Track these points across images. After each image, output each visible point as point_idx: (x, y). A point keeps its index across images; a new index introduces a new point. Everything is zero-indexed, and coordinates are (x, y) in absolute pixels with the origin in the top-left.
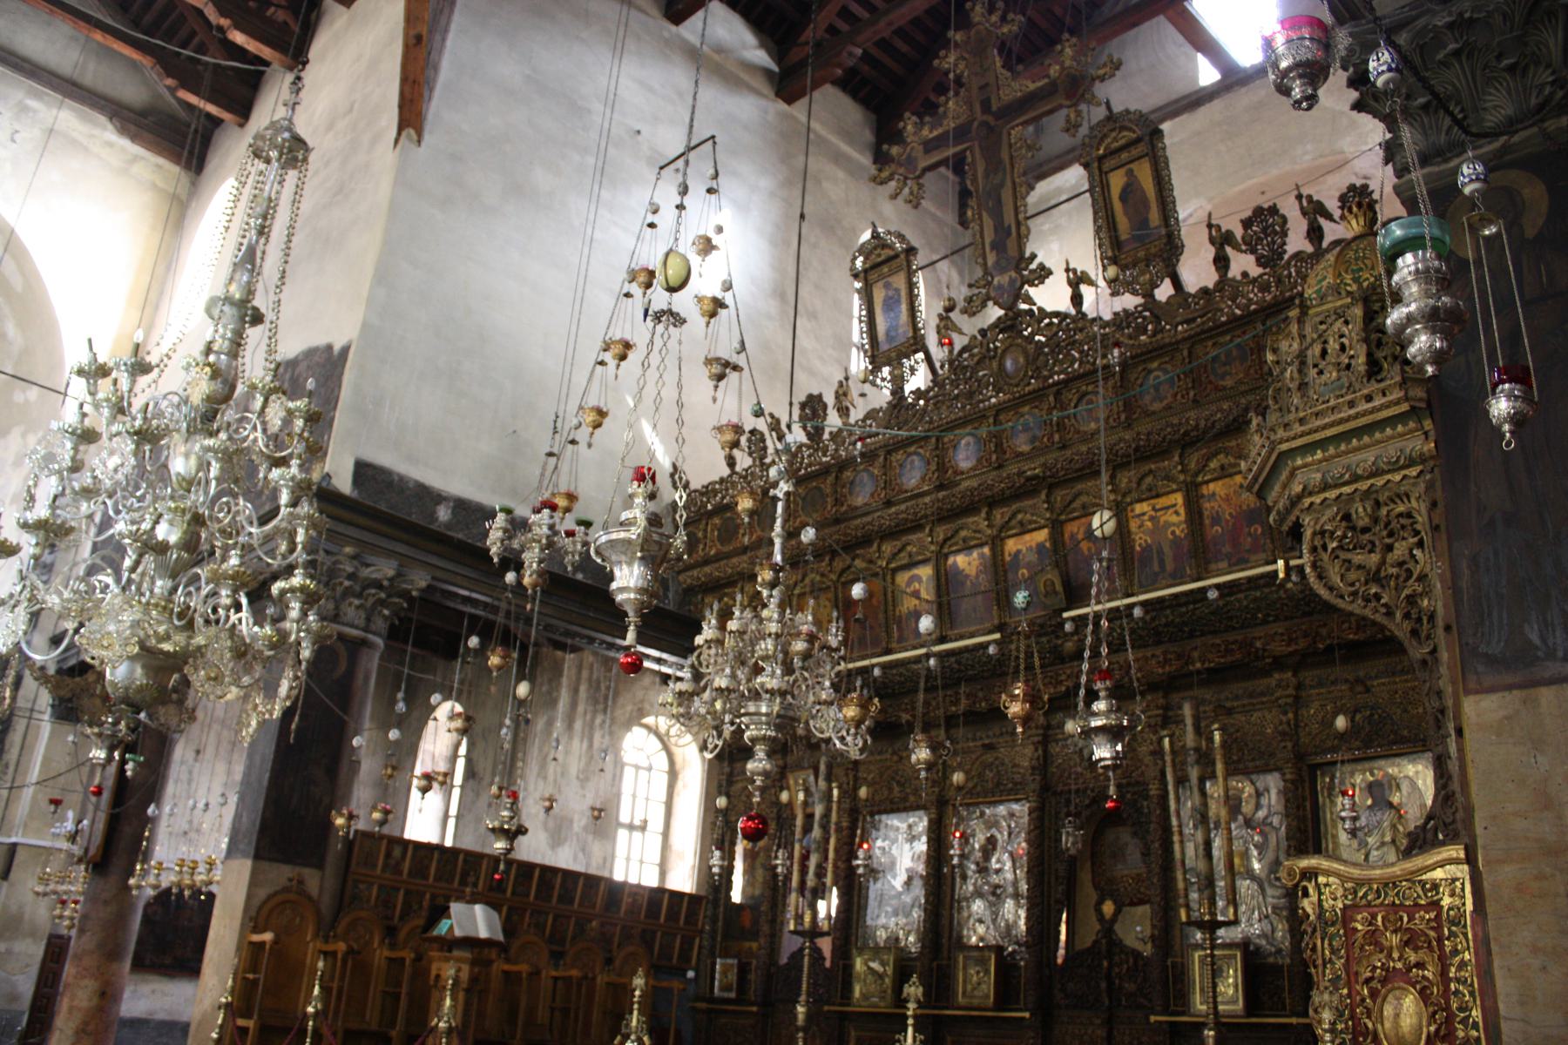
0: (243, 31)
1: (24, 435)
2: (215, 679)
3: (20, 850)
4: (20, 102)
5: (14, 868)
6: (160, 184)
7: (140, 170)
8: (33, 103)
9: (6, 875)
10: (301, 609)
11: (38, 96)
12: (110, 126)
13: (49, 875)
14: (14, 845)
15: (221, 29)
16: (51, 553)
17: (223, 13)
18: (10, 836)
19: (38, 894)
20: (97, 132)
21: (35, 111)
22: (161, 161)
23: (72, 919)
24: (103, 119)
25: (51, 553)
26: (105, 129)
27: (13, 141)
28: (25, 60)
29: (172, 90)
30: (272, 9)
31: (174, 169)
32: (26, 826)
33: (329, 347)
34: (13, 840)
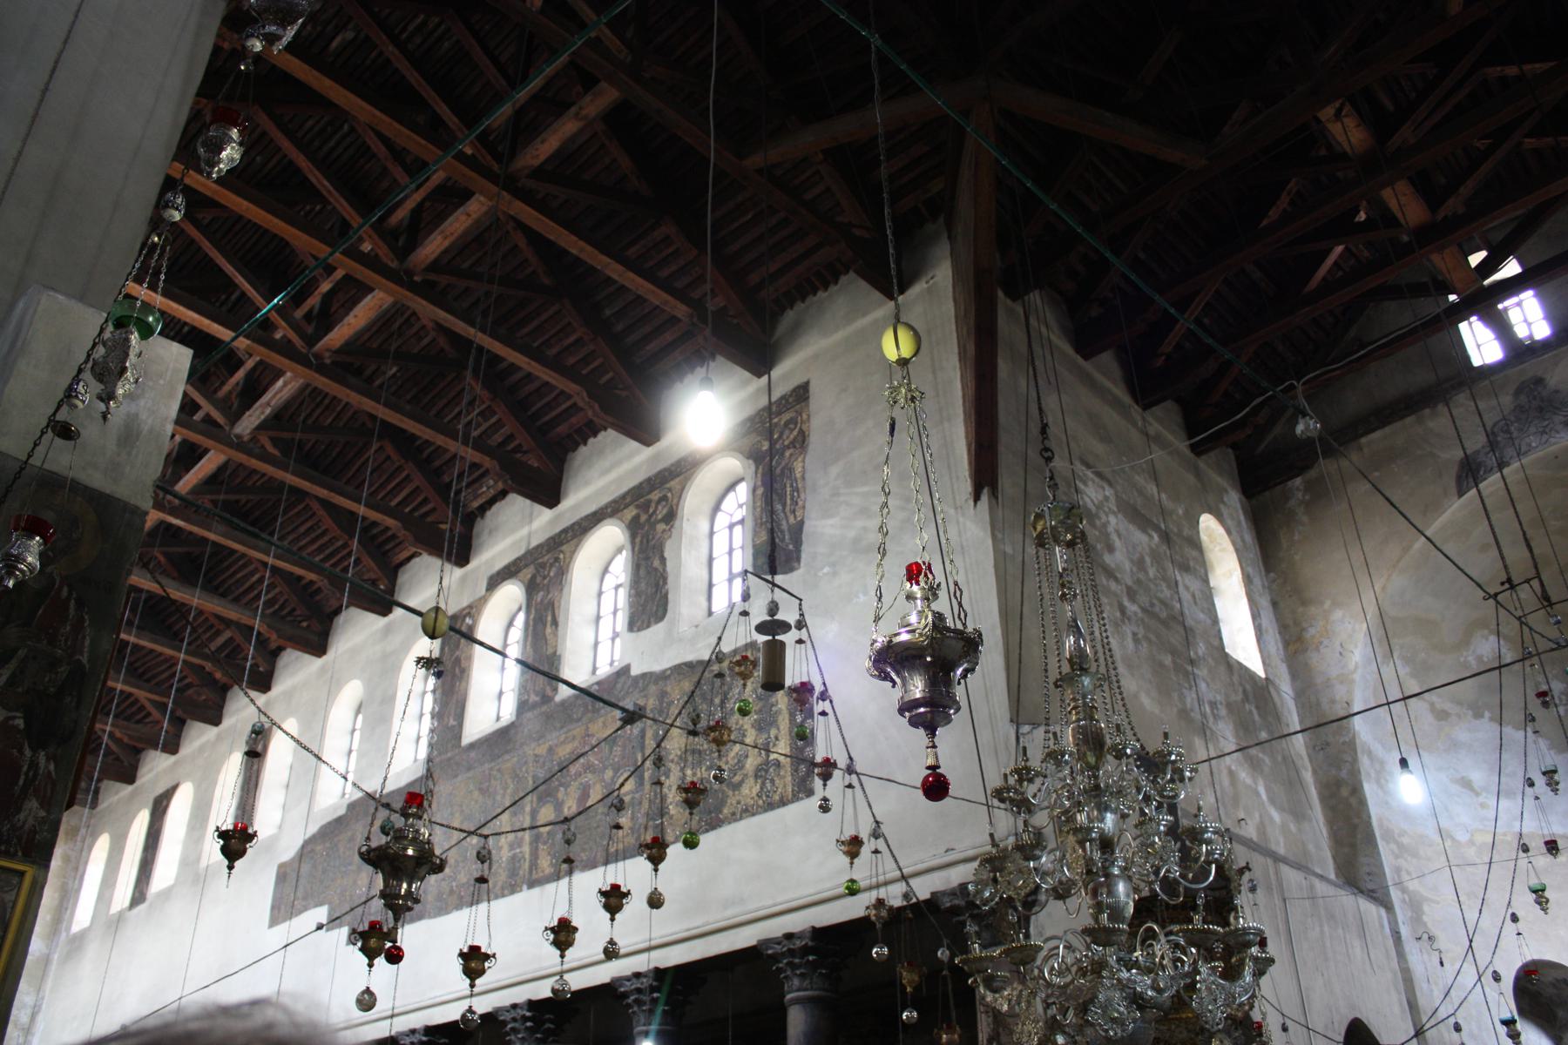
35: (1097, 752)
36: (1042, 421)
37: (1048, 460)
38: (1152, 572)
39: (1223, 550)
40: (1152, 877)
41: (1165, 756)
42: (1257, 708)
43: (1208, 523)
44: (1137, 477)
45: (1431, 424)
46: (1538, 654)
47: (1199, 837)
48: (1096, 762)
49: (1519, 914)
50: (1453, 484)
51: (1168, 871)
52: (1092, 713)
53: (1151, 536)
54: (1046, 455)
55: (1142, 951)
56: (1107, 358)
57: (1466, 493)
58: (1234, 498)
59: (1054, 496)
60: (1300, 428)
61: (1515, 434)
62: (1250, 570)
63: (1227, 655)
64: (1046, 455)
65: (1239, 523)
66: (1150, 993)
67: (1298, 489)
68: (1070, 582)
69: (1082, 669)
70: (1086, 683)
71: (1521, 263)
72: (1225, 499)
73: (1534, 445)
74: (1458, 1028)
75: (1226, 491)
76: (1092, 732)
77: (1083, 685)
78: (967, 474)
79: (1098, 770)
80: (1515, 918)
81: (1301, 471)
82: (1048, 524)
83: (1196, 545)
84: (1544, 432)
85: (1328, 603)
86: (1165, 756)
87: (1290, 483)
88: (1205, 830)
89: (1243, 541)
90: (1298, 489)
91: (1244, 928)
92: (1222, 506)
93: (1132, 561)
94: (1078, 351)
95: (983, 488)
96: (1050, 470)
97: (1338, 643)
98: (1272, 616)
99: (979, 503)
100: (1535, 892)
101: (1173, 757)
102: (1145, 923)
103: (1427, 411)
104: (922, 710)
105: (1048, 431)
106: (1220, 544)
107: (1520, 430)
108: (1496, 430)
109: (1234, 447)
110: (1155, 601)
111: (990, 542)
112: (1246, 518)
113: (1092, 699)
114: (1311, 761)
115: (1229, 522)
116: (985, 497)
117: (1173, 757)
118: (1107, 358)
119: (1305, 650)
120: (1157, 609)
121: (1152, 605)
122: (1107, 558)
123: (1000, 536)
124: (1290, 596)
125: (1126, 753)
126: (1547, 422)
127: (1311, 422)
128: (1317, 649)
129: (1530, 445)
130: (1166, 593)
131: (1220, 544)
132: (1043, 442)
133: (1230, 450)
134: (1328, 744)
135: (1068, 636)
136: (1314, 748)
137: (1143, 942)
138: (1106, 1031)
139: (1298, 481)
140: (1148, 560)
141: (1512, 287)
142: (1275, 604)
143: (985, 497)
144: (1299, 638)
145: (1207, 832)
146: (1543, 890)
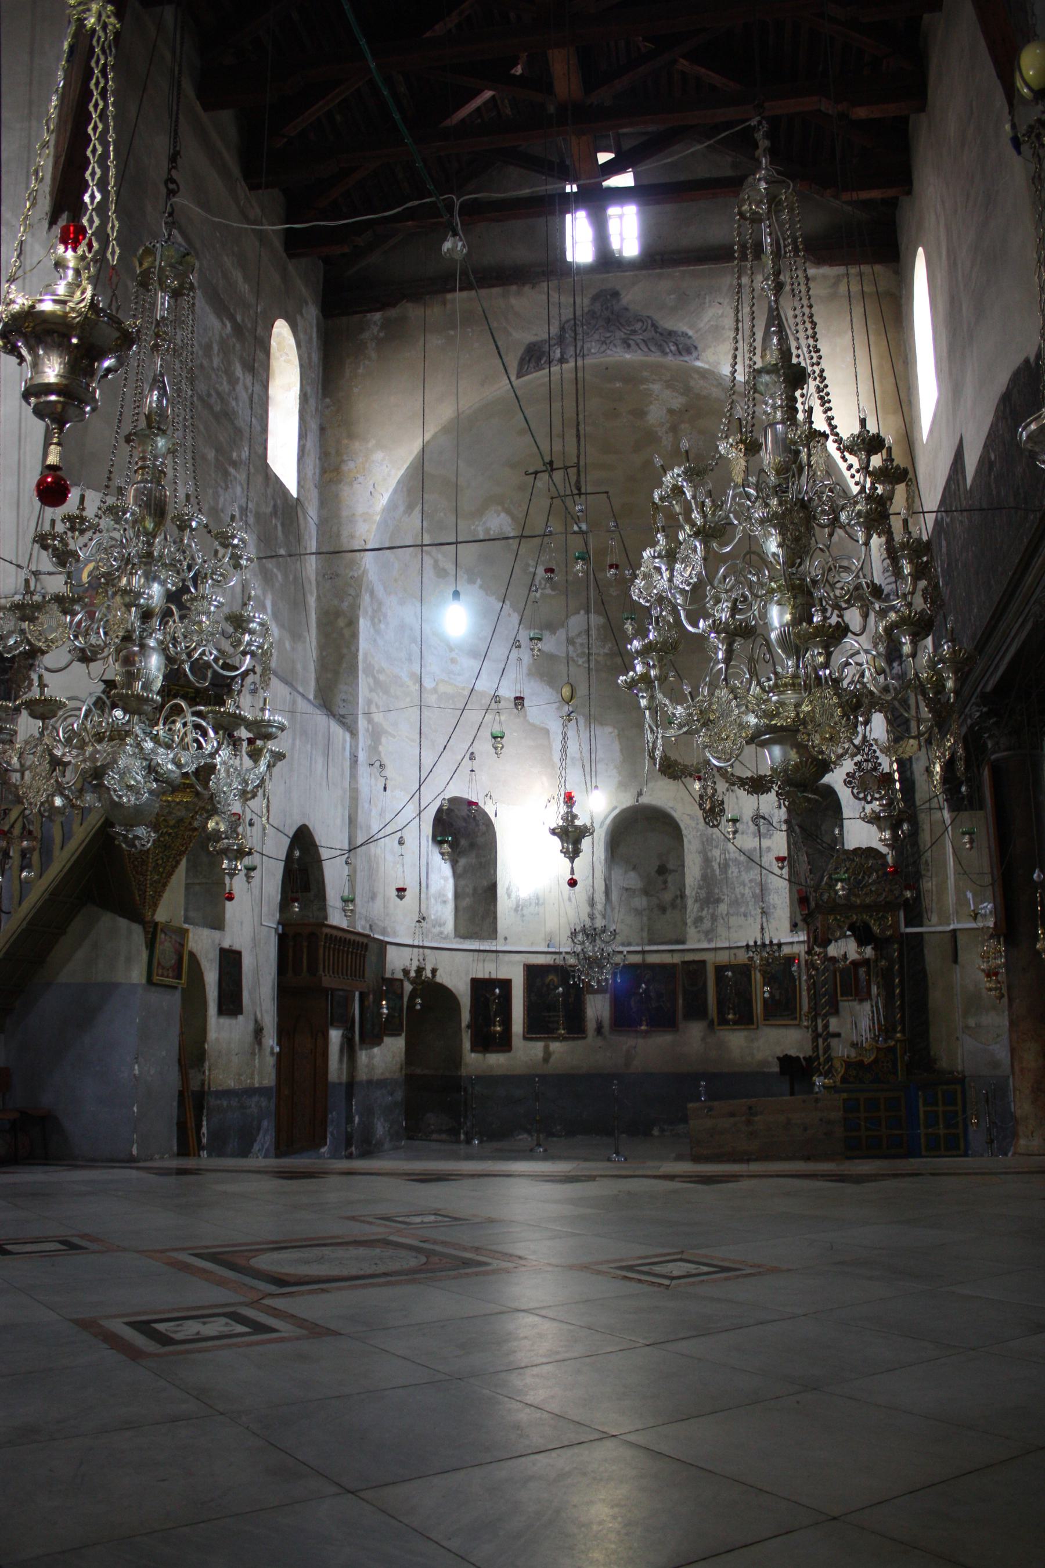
2: (831, 739)
3: (959, 936)
5: (960, 952)
10: (912, 642)
14: (954, 931)
18: (949, 924)
25: (900, 664)
32: (957, 913)
33: (1027, 361)
34: (952, 927)
35: (157, 519)
36: (175, 147)
37: (171, 193)
38: (216, 361)
39: (288, 361)
40: (184, 657)
41: (228, 538)
42: (283, 525)
44: (226, 259)
45: (513, 301)
47: (244, 625)
48: (154, 529)
49: (477, 755)
51: (203, 653)
52: (160, 477)
54: (172, 186)
55: (164, 724)
56: (227, 116)
57: (523, 376)
58: (312, 312)
59: (170, 235)
60: (447, 245)
62: (309, 389)
63: (267, 466)
64: (172, 186)
65: (311, 339)
66: (170, 766)
67: (375, 323)
68: (165, 333)
69: (159, 429)
70: (160, 444)
72: (304, 311)
73: (593, 351)
74: (401, 842)
75: (307, 304)
76: (156, 497)
77: (157, 445)
79: (154, 537)
80: (472, 757)
82: (157, 263)
83: (264, 344)
84: (604, 342)
85: (372, 443)
86: (228, 538)
88: (251, 620)
89: (310, 358)
90: (375, 323)
91: (269, 721)
92: (299, 317)
95: (62, 211)
96: (171, 205)
97: (371, 483)
100: (495, 738)
101: (236, 541)
102: (175, 697)
103: (514, 288)
104: (53, 398)
105: (179, 160)
106: (287, 354)
108: (566, 326)
110: (212, 392)
112: (318, 337)
113: (162, 463)
115: (302, 336)
117: (236, 541)
118: (227, 116)
119: (340, 481)
120: (213, 400)
121: (209, 395)
124: (339, 426)
125: (191, 526)
126: (608, 335)
127: (460, 244)
128: (351, 484)
129: (589, 350)
130: (225, 387)
131: (287, 354)
132: (169, 171)
134: (337, 575)
135: (151, 390)
136: (324, 576)
137: (166, 719)
138: (120, 797)
139: (377, 316)
140: (216, 348)
141: (621, 195)
142: (322, 429)
144: (337, 470)
145: (253, 622)
146: (502, 738)
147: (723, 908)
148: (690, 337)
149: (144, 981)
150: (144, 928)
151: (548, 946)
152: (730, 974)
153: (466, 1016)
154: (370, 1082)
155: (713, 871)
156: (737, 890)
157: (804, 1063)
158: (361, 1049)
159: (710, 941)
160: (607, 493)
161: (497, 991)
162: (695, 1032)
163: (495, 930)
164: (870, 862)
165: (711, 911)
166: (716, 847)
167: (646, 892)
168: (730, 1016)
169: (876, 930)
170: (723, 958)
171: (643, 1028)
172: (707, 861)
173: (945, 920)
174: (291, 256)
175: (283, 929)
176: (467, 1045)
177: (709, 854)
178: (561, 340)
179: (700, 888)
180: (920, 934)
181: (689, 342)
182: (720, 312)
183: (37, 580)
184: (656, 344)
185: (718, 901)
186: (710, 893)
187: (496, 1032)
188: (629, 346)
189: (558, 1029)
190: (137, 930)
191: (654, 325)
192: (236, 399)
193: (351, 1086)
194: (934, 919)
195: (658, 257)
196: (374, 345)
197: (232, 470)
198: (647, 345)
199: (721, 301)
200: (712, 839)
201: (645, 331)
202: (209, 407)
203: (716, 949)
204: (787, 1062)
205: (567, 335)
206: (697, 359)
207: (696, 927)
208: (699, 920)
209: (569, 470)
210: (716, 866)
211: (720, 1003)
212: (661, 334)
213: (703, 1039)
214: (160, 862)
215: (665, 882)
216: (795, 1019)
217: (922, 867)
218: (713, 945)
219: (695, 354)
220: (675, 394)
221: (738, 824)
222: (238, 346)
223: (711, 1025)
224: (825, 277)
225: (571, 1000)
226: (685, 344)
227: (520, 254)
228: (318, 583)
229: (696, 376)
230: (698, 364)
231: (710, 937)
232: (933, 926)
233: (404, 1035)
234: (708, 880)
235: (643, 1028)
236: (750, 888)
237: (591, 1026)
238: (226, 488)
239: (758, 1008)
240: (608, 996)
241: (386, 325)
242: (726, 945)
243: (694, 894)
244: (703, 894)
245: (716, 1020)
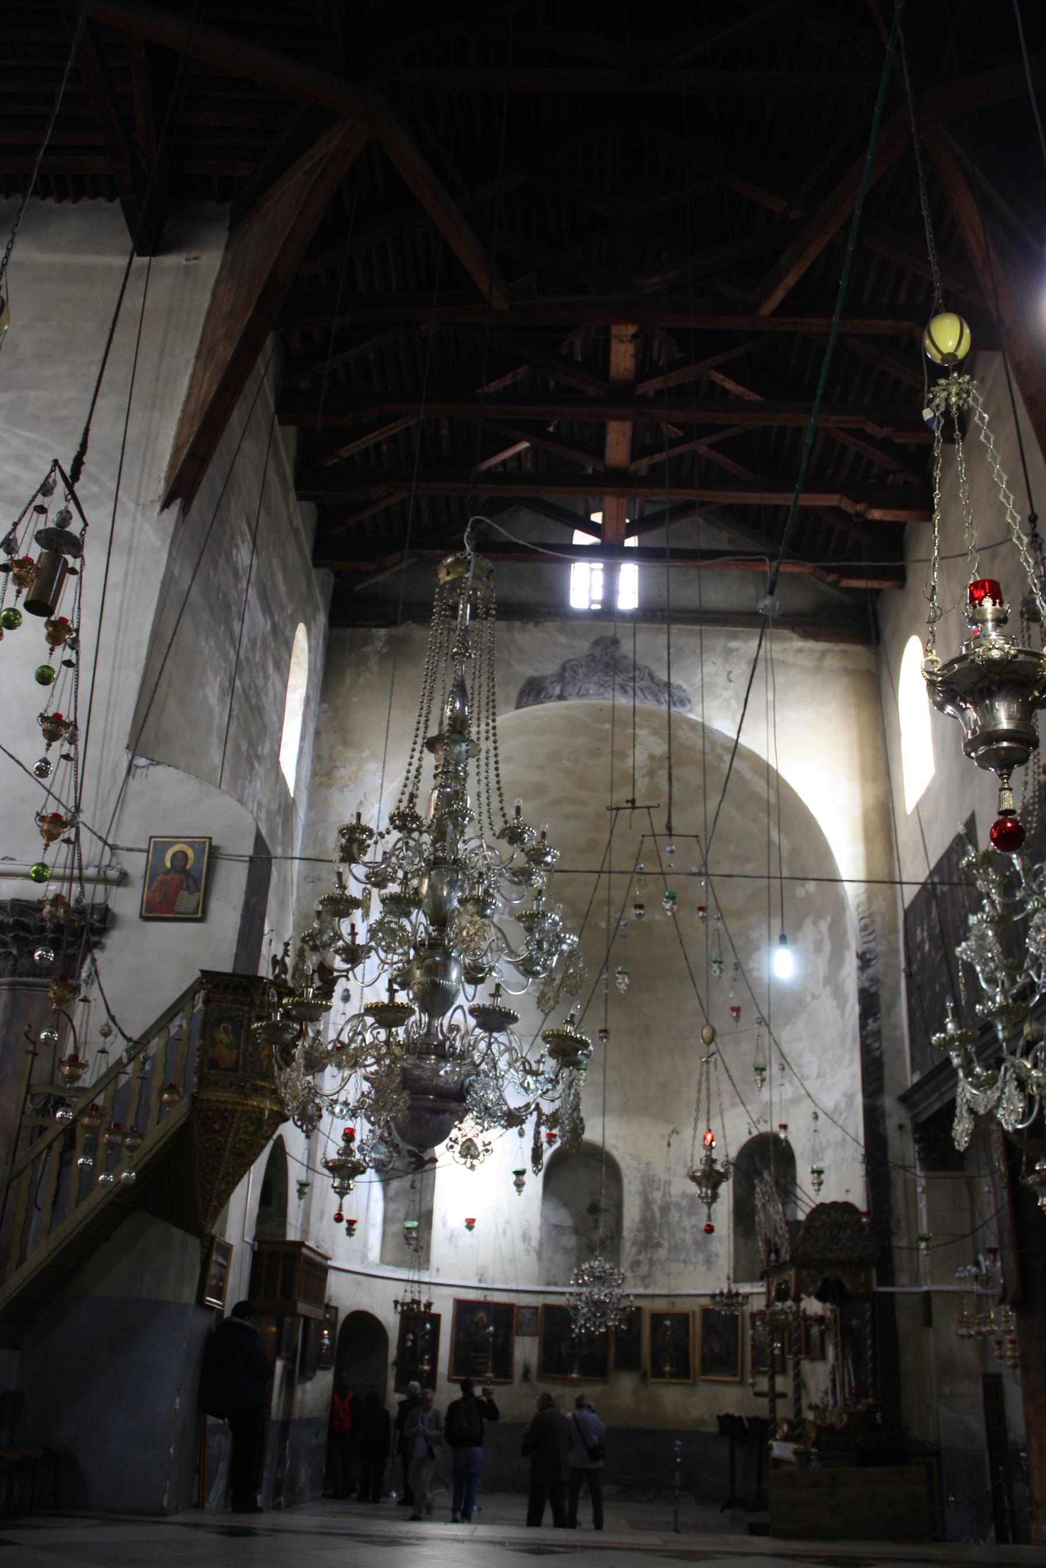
0: (878, 507)
1: (815, 923)
4: (725, 647)
6: (850, 666)
7: (829, 662)
8: (733, 644)
9: (928, 1322)
11: (735, 637)
12: (794, 636)
13: (968, 1318)
14: (927, 1293)
15: (859, 515)
16: (875, 1021)
17: (857, 501)
18: (920, 1286)
19: (962, 1337)
20: (786, 645)
21: (737, 650)
22: (843, 646)
23: (1013, 1357)
24: (787, 632)
25: (875, 1021)
26: (791, 640)
27: (730, 681)
28: (716, 612)
29: (834, 585)
30: (891, 477)
31: (859, 649)
34: (925, 1288)
43: (301, 632)
45: (517, 636)
46: (634, 872)
50: (515, 695)
53: (266, 621)
56: (292, 431)
58: (322, 619)
61: (580, 677)
62: (311, 692)
63: (278, 763)
65: (317, 646)
67: (379, 639)
71: (640, 541)
73: (591, 692)
78: (163, 475)
81: (389, 622)
84: (602, 685)
85: (366, 753)
87: (374, 630)
89: (315, 664)
90: (379, 639)
92: (313, 624)
93: (249, 638)
94: (278, 410)
95: (177, 498)
97: (362, 792)
98: (311, 743)
99: (166, 510)
103: (518, 624)
107: (586, 675)
108: (567, 666)
109: (338, 574)
111: (165, 555)
112: (324, 644)
114: (298, 889)
115: (313, 642)
116: (175, 508)
118: (292, 431)
119: (330, 786)
120: (252, 693)
121: (250, 688)
122: (236, 626)
123: (174, 554)
124: (335, 732)
126: (607, 679)
128: (342, 790)
129: (588, 690)
133: (332, 575)
134: (319, 879)
136: (305, 878)
139: (382, 632)
140: (259, 643)
142: (317, 733)
143: (175, 508)
144: (329, 774)
147: (662, 1253)
148: (684, 691)
149: (193, 1301)
150: (202, 1242)
151: (480, 1281)
152: (668, 1323)
153: (393, 1352)
154: (301, 1420)
155: (653, 1214)
156: (678, 1235)
157: (746, 1423)
158: (299, 1383)
159: (646, 1286)
160: (697, 836)
161: (428, 1326)
162: (626, 1384)
163: (428, 1261)
164: (847, 1217)
165: (649, 1255)
166: (658, 1189)
167: (576, 1231)
168: (667, 1369)
169: (849, 1286)
170: (660, 1305)
171: (574, 1375)
172: (647, 1203)
173: (916, 1280)
174: (317, 564)
175: (259, 1246)
176: (391, 1383)
177: (650, 1196)
178: (561, 677)
179: (639, 1230)
180: (892, 1294)
181: (683, 694)
182: (714, 670)
183: (113, 855)
184: (652, 693)
185: (658, 1245)
186: (649, 1237)
187: (423, 1371)
188: (626, 692)
189: (486, 1372)
190: (194, 1244)
191: (651, 676)
192: (266, 695)
193: (286, 1423)
194: (904, 1278)
195: (659, 614)
196: (376, 658)
197: (256, 764)
198: (643, 693)
199: (715, 660)
200: (653, 1181)
201: (642, 679)
202: (248, 698)
203: (653, 1296)
204: (728, 1423)
205: (567, 674)
206: (690, 711)
207: (633, 1271)
208: (635, 1264)
209: (652, 810)
210: (656, 1209)
211: (655, 1353)
212: (658, 685)
213: (635, 1392)
214: (231, 1170)
215: (596, 1222)
216: (736, 1375)
217: (893, 1224)
218: (649, 1291)
219: (688, 707)
220: (659, 741)
221: (823, 1176)
222: (273, 644)
223: (644, 1377)
224: (811, 651)
225: (500, 1340)
226: (679, 697)
227: (525, 593)
228: (298, 884)
229: (685, 727)
230: (692, 716)
231: (647, 1282)
232: (903, 1286)
233: (333, 1369)
234: (647, 1223)
235: (574, 1375)
236: (691, 1234)
237: (518, 1370)
238: (251, 782)
239: (696, 1359)
240: (537, 1339)
241: (389, 641)
242: (665, 1291)
243: (632, 1236)
244: (641, 1237)
245: (649, 1373)
